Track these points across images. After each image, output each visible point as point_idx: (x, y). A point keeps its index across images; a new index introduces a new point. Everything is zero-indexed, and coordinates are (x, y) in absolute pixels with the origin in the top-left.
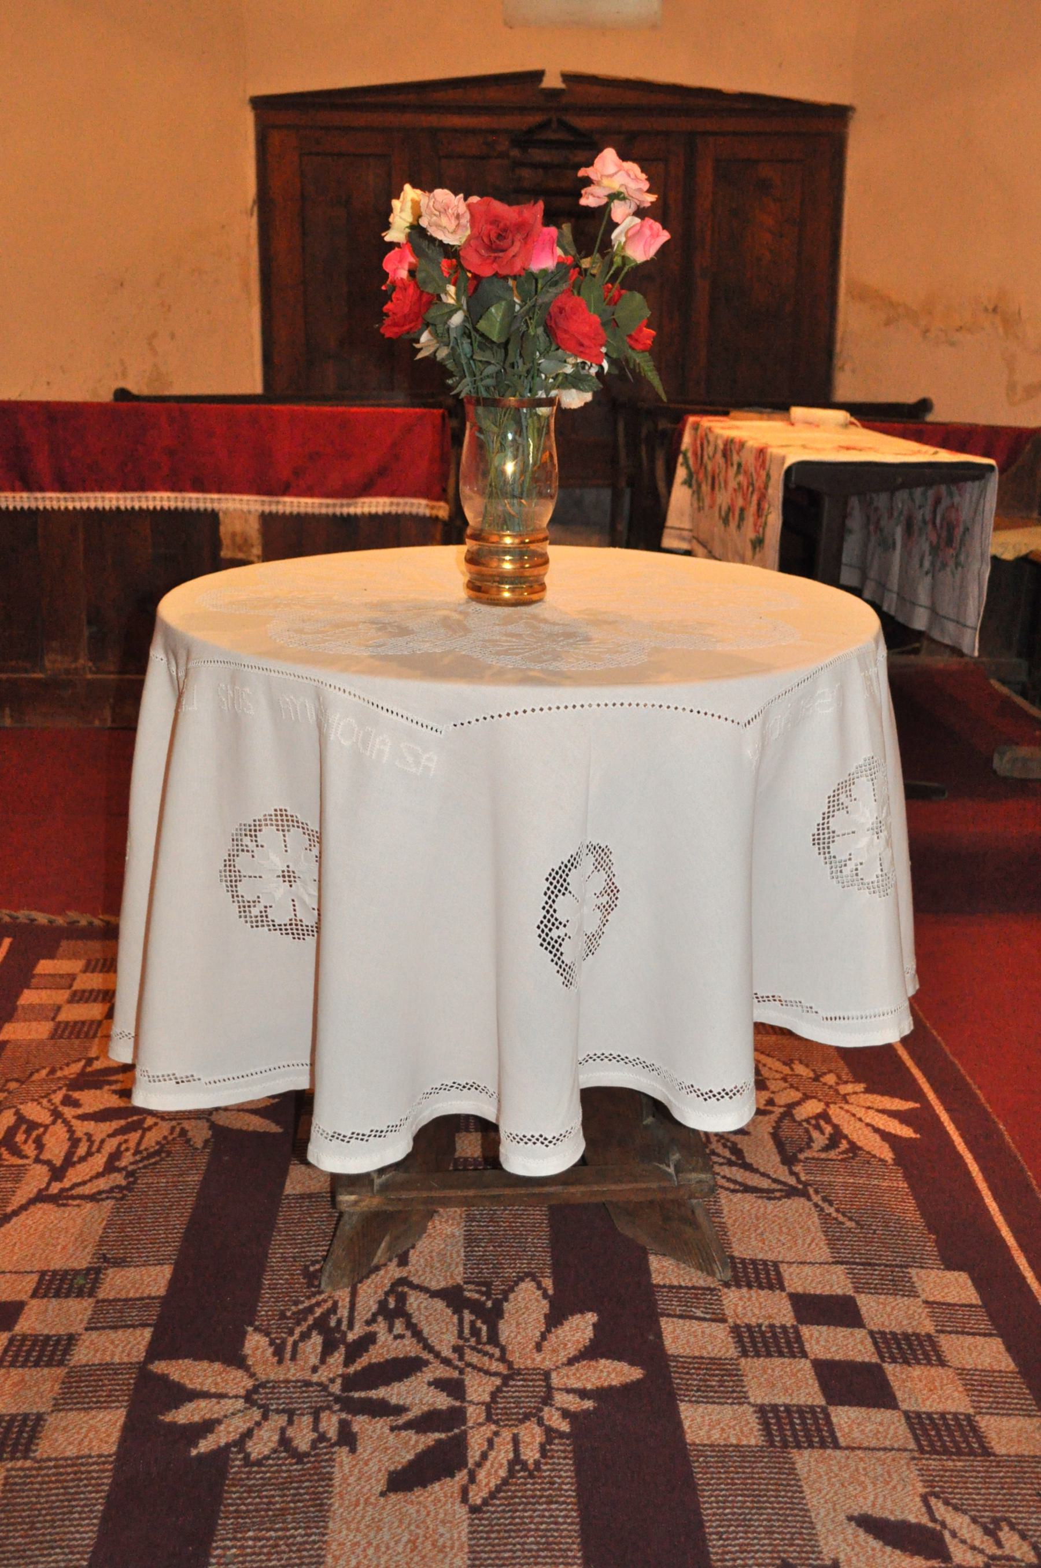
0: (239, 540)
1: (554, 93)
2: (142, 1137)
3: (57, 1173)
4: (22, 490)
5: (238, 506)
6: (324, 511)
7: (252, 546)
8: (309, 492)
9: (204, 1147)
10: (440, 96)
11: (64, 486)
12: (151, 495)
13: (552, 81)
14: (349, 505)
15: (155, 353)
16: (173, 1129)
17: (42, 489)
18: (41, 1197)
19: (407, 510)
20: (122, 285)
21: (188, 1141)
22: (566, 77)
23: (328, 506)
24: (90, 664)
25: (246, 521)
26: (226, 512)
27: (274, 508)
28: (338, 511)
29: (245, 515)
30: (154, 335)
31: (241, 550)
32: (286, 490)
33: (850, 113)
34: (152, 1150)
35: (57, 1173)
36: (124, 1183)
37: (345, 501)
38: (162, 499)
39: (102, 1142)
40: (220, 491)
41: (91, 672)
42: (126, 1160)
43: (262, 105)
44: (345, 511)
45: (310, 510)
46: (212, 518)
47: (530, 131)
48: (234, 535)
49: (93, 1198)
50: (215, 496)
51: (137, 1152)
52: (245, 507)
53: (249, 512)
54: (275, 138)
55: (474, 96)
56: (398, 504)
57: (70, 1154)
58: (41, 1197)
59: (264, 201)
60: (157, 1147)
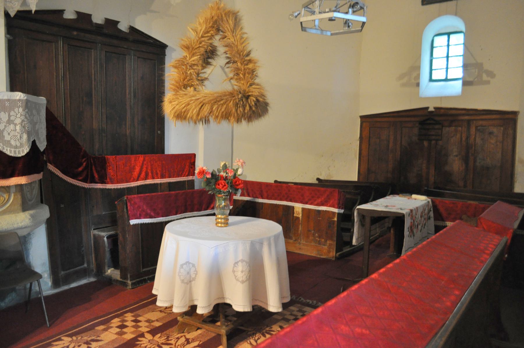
1: (432, 112)
4: (261, 199)
8: (311, 204)
10: (401, 114)
11: (268, 198)
12: (283, 202)
13: (431, 109)
15: (329, 170)
17: (264, 199)
20: (322, 156)
22: (435, 108)
25: (299, 209)
29: (299, 208)
30: (330, 166)
31: (298, 214)
32: (306, 203)
33: (518, 113)
37: (318, 207)
38: (289, 203)
43: (362, 117)
44: (318, 209)
45: (311, 208)
47: (424, 121)
48: (297, 211)
50: (294, 203)
53: (300, 207)
54: (364, 124)
55: (411, 113)
59: (361, 138)
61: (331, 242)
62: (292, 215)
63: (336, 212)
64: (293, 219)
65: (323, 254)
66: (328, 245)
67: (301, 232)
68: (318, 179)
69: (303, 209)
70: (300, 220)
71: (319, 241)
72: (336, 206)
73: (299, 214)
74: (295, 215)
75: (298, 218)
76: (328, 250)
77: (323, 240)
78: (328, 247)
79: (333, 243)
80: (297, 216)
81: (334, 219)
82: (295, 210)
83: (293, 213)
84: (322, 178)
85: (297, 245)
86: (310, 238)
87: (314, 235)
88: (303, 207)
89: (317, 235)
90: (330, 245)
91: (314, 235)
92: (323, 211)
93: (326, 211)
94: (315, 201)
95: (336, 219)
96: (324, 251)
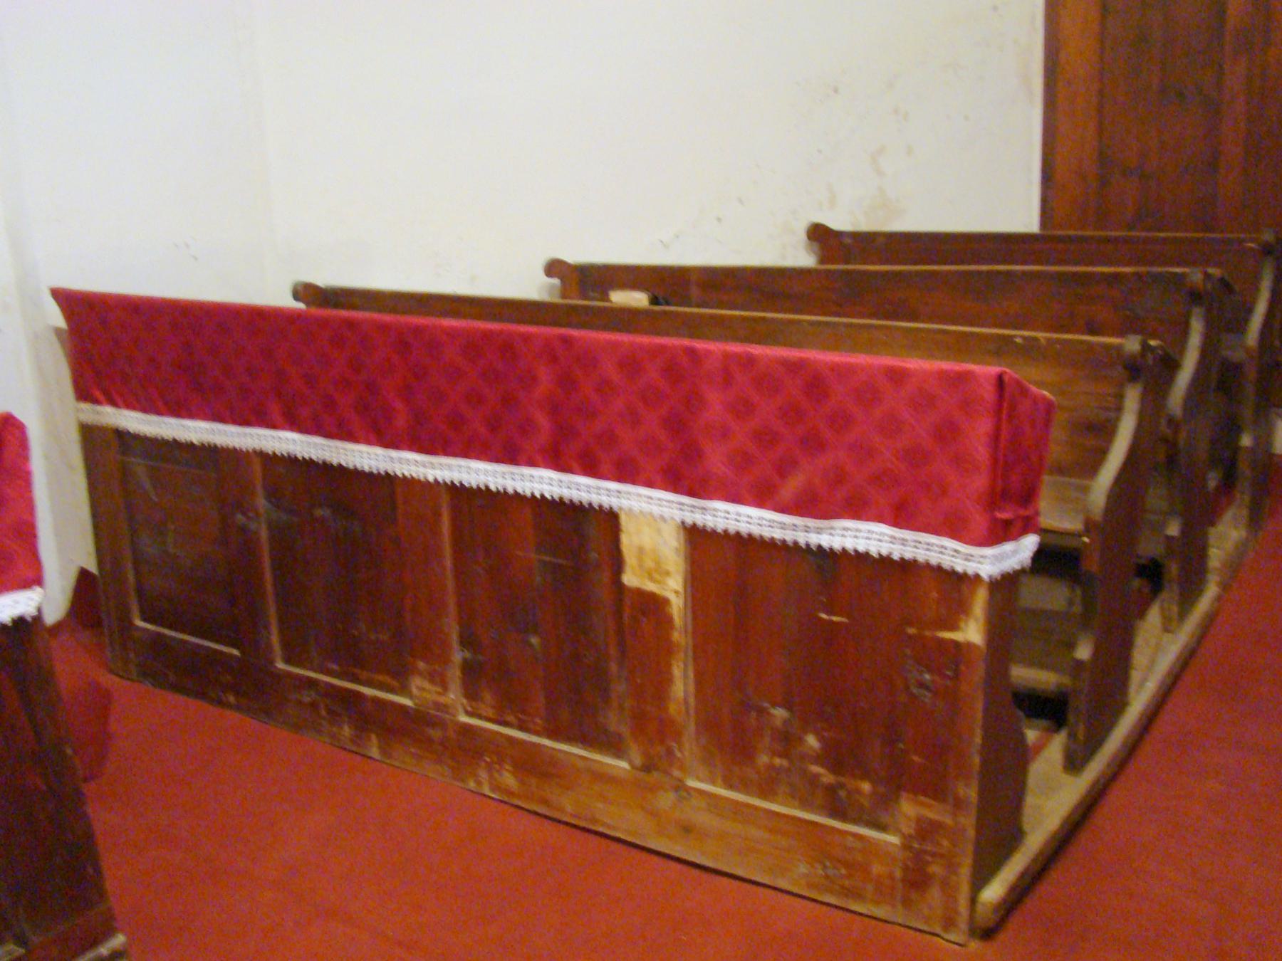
0: (649, 564)
5: (646, 507)
6: (778, 534)
7: (668, 573)
14: (819, 531)
19: (921, 555)
23: (783, 526)
24: (465, 701)
25: (659, 531)
26: (630, 512)
27: (699, 519)
28: (802, 538)
31: (652, 579)
40: (621, 479)
41: (469, 714)
45: (756, 531)
46: (610, 519)
48: (641, 550)
50: (613, 485)
52: (656, 510)
53: (663, 518)
56: (904, 542)
61: (935, 812)
62: (605, 577)
63: (977, 577)
64: (618, 614)
65: (870, 887)
66: (908, 829)
67: (687, 710)
68: (819, 234)
69: (696, 536)
70: (670, 620)
71: (831, 790)
72: (979, 521)
73: (658, 572)
74: (630, 579)
75: (653, 605)
76: (906, 869)
77: (866, 787)
78: (906, 847)
79: (948, 821)
80: (650, 587)
81: (954, 627)
82: (625, 539)
83: (616, 562)
84: (840, 222)
85: (666, 800)
86: (763, 759)
87: (786, 741)
88: (689, 521)
89: (812, 741)
90: (927, 830)
91: (786, 741)
92: (862, 558)
93: (885, 562)
94: (784, 469)
95: (972, 632)
96: (877, 869)
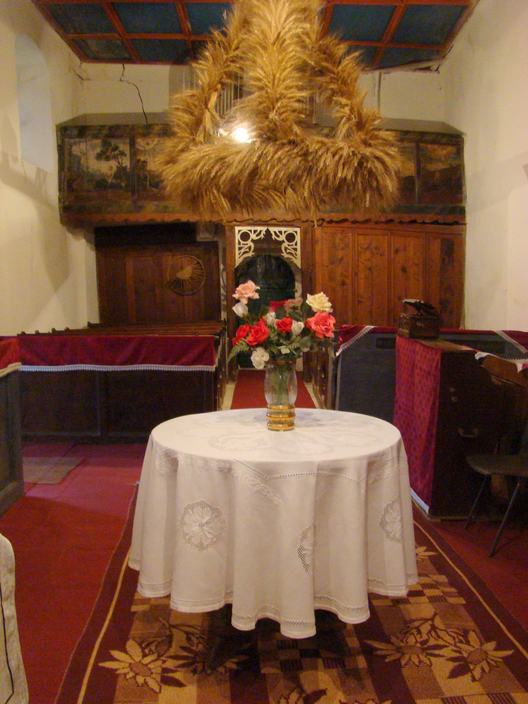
2: (416, 639)
3: (434, 628)
9: (389, 636)
16: (407, 642)
18: (432, 619)
21: (397, 638)
34: (408, 635)
35: (434, 628)
36: (408, 625)
39: (429, 637)
42: (415, 631)
49: (414, 621)
51: (413, 634)
57: (436, 632)
58: (432, 619)
60: (407, 636)
